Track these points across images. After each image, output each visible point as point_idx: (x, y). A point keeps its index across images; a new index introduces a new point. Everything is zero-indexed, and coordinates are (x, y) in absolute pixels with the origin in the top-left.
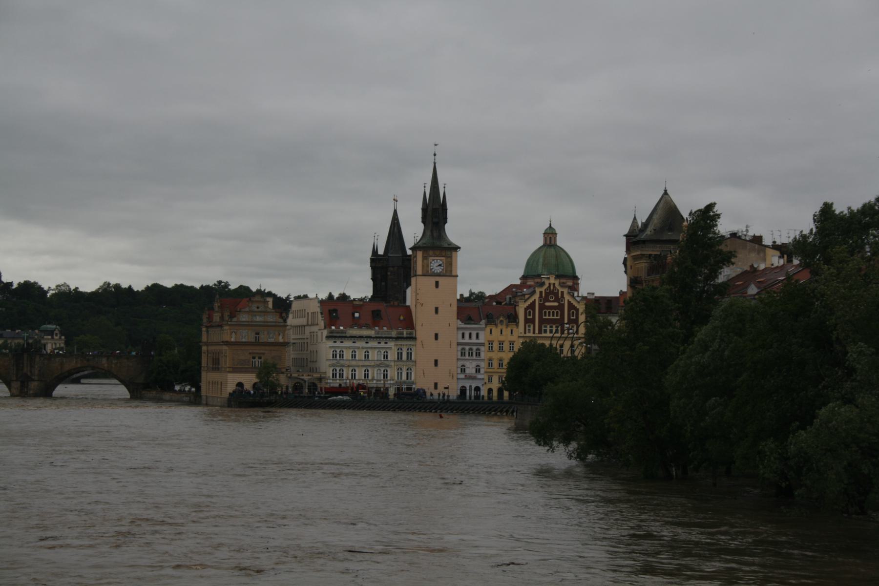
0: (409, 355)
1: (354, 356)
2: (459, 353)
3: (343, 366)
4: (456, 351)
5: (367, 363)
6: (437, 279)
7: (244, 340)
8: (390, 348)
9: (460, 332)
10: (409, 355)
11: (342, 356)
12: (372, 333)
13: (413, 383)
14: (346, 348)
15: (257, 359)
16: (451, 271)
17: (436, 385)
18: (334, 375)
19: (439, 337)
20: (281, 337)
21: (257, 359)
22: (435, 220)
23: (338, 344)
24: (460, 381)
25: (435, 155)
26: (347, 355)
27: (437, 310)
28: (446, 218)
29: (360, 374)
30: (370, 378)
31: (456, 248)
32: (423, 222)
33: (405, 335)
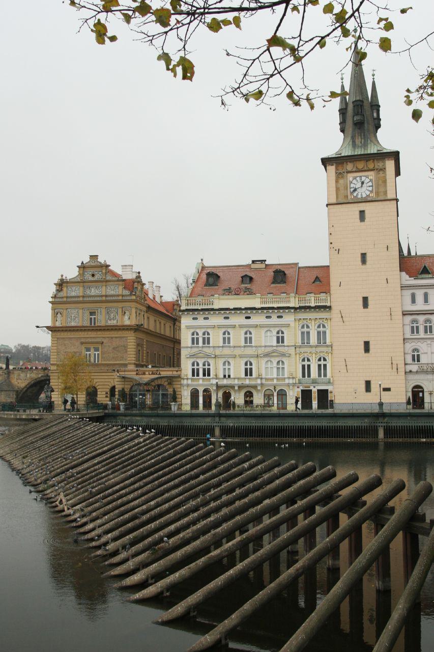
0: (321, 336)
1: (226, 340)
2: (408, 329)
3: (208, 356)
4: (399, 327)
5: (249, 351)
6: (362, 207)
7: (73, 324)
8: (288, 326)
9: (408, 294)
10: (321, 336)
11: (207, 341)
12: (255, 302)
14: (214, 327)
15: (92, 352)
16: (385, 193)
17: (368, 385)
18: (195, 373)
20: (126, 317)
21: (92, 352)
24: (410, 377)
27: (364, 257)
29: (237, 370)
30: (254, 375)
31: (395, 155)
32: (342, 131)
33: (313, 305)
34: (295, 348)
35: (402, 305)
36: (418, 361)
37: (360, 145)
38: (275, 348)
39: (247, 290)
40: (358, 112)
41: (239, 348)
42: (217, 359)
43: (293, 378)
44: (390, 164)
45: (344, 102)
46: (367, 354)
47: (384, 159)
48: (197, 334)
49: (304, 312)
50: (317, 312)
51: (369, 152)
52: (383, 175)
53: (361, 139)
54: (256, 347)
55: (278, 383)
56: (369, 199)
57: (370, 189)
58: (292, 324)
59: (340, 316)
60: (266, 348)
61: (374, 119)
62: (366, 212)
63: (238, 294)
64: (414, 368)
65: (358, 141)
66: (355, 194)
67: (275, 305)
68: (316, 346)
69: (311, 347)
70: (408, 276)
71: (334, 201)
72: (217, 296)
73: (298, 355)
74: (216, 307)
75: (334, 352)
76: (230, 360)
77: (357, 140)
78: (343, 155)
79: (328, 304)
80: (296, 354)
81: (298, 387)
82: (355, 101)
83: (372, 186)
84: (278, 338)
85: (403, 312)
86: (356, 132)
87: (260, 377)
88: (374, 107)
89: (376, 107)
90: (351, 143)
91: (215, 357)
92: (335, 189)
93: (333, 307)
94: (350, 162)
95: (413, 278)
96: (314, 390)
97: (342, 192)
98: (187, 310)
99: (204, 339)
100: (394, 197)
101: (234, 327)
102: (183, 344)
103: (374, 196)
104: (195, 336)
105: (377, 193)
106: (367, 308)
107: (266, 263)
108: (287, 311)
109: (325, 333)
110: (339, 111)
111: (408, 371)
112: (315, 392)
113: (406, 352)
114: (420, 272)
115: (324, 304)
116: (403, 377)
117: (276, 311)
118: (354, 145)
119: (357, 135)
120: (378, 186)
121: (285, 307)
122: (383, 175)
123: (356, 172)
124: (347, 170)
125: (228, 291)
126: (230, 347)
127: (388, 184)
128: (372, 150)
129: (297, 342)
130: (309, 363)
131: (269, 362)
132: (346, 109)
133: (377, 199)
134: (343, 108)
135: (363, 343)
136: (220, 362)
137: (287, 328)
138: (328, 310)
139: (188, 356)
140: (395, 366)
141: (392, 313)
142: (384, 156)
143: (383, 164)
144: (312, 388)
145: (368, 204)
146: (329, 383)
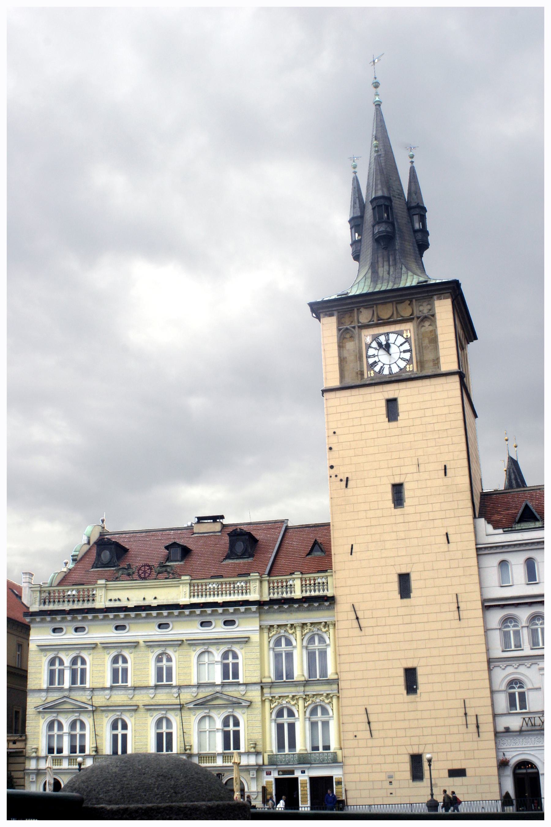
2: (496, 638)
3: (81, 710)
6: (391, 391)
8: (246, 641)
11: (78, 676)
12: (179, 593)
13: (334, 761)
14: (94, 647)
16: (437, 361)
17: (416, 761)
19: (414, 584)
22: (382, 228)
23: (69, 636)
25: (376, 85)
26: (99, 670)
27: (398, 491)
28: (424, 232)
31: (453, 290)
32: (356, 257)
34: (262, 688)
35: (481, 588)
36: (523, 706)
37: (386, 275)
38: (218, 689)
39: (164, 569)
40: (381, 217)
41: (143, 692)
42: (98, 716)
43: (257, 754)
44: (444, 309)
45: (358, 205)
46: (412, 697)
47: (431, 297)
48: (61, 662)
49: (281, 611)
50: (309, 610)
51: (402, 286)
52: (431, 328)
53: (389, 266)
54: (180, 687)
55: (225, 764)
56: (404, 375)
57: (407, 356)
58: (255, 637)
59: (355, 617)
60: (201, 689)
61: (415, 231)
62: (400, 401)
63: (145, 578)
64: (515, 723)
65: (382, 271)
66: (377, 369)
67: (219, 599)
68: (306, 683)
69: (297, 684)
70: (490, 528)
71: (336, 383)
72: (102, 582)
73: (267, 704)
74: (100, 604)
75: (343, 694)
76: (127, 717)
77: (380, 270)
78: (350, 295)
79: (329, 593)
80: (263, 702)
81: (269, 774)
82: (375, 199)
83: (410, 351)
84: (225, 667)
85: (484, 601)
86: (380, 255)
87: (188, 752)
88: (413, 211)
89: (417, 211)
90: (369, 275)
91: (95, 711)
92: (337, 360)
93: (339, 599)
94: (366, 307)
95: (501, 531)
96: (303, 778)
97: (352, 366)
98: (42, 613)
99: (74, 673)
100: (454, 367)
101: (136, 645)
102: (31, 684)
103: (415, 370)
104: (57, 666)
105: (421, 364)
106: (410, 597)
107: (225, 522)
108: (242, 609)
109: (323, 654)
110: (350, 221)
111: (501, 728)
112: (304, 783)
113: (496, 688)
114: (517, 519)
115: (321, 593)
116: (492, 744)
117: (220, 610)
118: (375, 277)
119: (380, 259)
120: (421, 349)
121: (239, 601)
122: (431, 328)
123: (377, 325)
124: (359, 322)
125: (126, 572)
126: (126, 688)
127: (441, 345)
128: (410, 280)
129: (267, 674)
130: (291, 720)
131: (207, 720)
132: (362, 217)
133: (420, 375)
134: (355, 215)
135: (402, 673)
136: (106, 722)
137: (243, 645)
138: (327, 604)
139: (41, 710)
140: (472, 720)
141: (460, 605)
142: (428, 291)
143: (429, 307)
144: (297, 774)
145: (402, 385)
146: (334, 761)
